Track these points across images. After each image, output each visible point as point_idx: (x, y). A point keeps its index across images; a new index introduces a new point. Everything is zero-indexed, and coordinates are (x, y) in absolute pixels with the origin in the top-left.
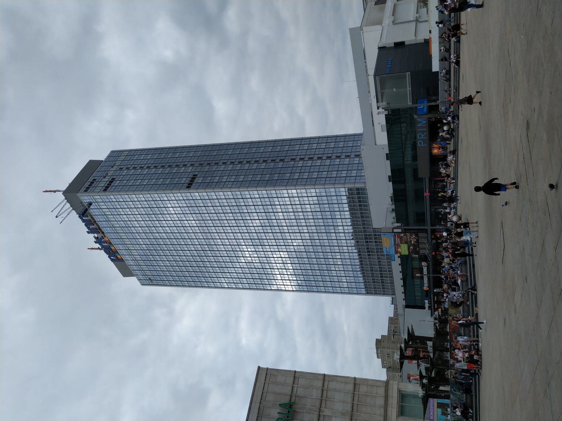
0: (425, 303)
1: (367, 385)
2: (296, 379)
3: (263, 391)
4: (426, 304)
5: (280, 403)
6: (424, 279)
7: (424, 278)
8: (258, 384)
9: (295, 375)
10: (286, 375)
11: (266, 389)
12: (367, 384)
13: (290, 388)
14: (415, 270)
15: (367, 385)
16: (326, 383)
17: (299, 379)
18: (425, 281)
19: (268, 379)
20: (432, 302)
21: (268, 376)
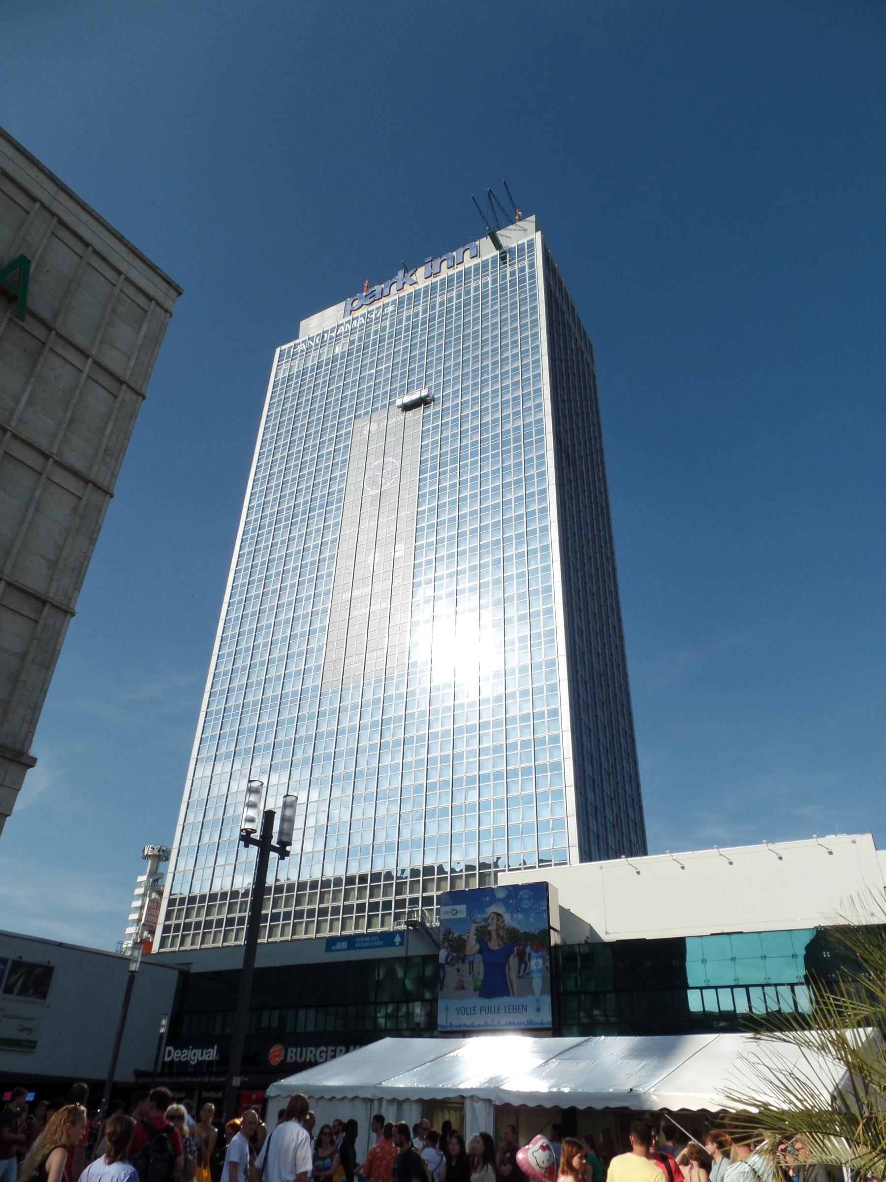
0: (203, 1044)
1: (23, 656)
2: (113, 386)
3: (90, 249)
4: (198, 1052)
5: (33, 267)
6: (323, 1048)
7: (330, 1048)
8: (122, 250)
9: (128, 386)
10: (133, 359)
11: (96, 262)
12: (30, 657)
13: (81, 340)
14: (396, 1005)
15: (23, 656)
16: (72, 484)
17: (109, 396)
18: (313, 1049)
19: (130, 291)
20: (206, 1080)
21: (141, 300)
